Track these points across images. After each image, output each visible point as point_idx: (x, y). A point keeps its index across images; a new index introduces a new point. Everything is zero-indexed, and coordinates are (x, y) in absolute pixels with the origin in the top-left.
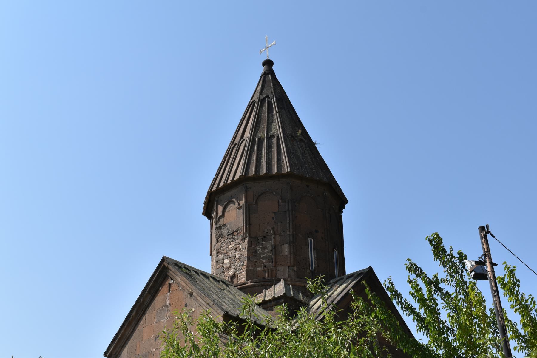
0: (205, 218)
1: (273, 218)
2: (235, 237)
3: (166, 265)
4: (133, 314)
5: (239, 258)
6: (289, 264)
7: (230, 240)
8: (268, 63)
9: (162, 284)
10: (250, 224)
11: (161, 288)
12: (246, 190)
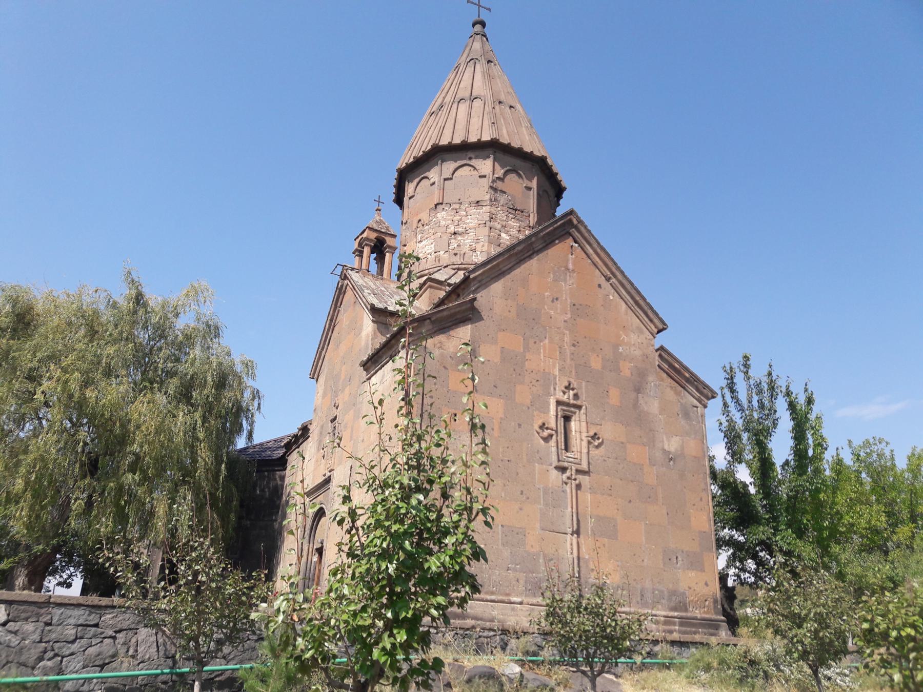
3: (575, 222)
11: (557, 242)
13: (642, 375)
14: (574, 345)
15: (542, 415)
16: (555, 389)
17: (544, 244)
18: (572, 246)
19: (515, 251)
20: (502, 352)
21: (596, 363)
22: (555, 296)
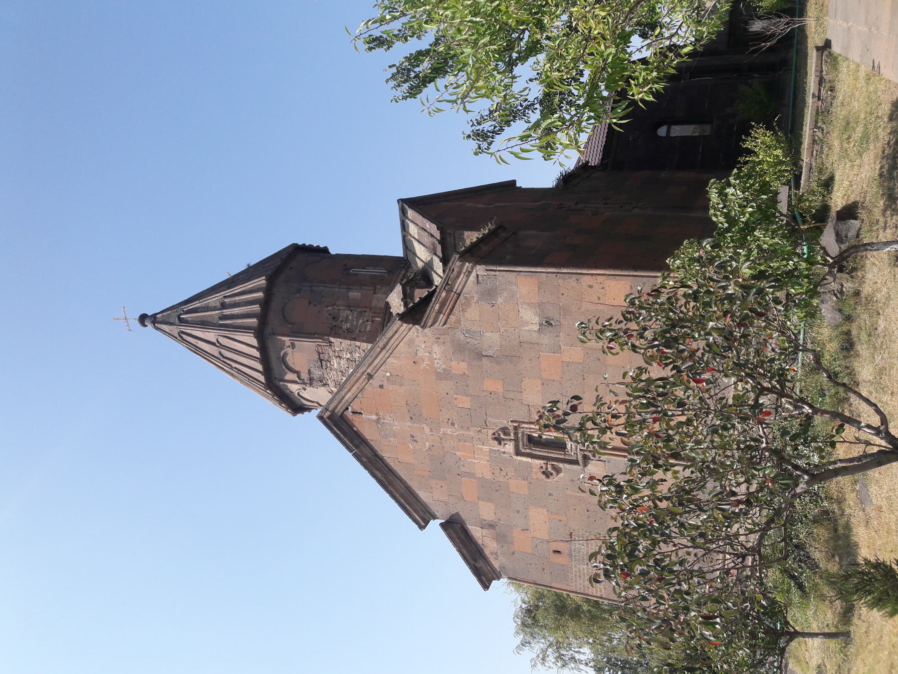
0: (299, 415)
1: (315, 306)
2: (326, 358)
3: (328, 414)
4: (379, 475)
5: (351, 353)
6: (372, 292)
7: (329, 365)
8: (143, 319)
9: (350, 426)
10: (315, 334)
11: (355, 429)
12: (274, 334)
13: (460, 349)
14: (453, 424)
15: (534, 470)
16: (504, 453)
17: (364, 444)
18: (352, 412)
19: (382, 479)
20: (483, 500)
21: (465, 402)
22: (409, 437)
